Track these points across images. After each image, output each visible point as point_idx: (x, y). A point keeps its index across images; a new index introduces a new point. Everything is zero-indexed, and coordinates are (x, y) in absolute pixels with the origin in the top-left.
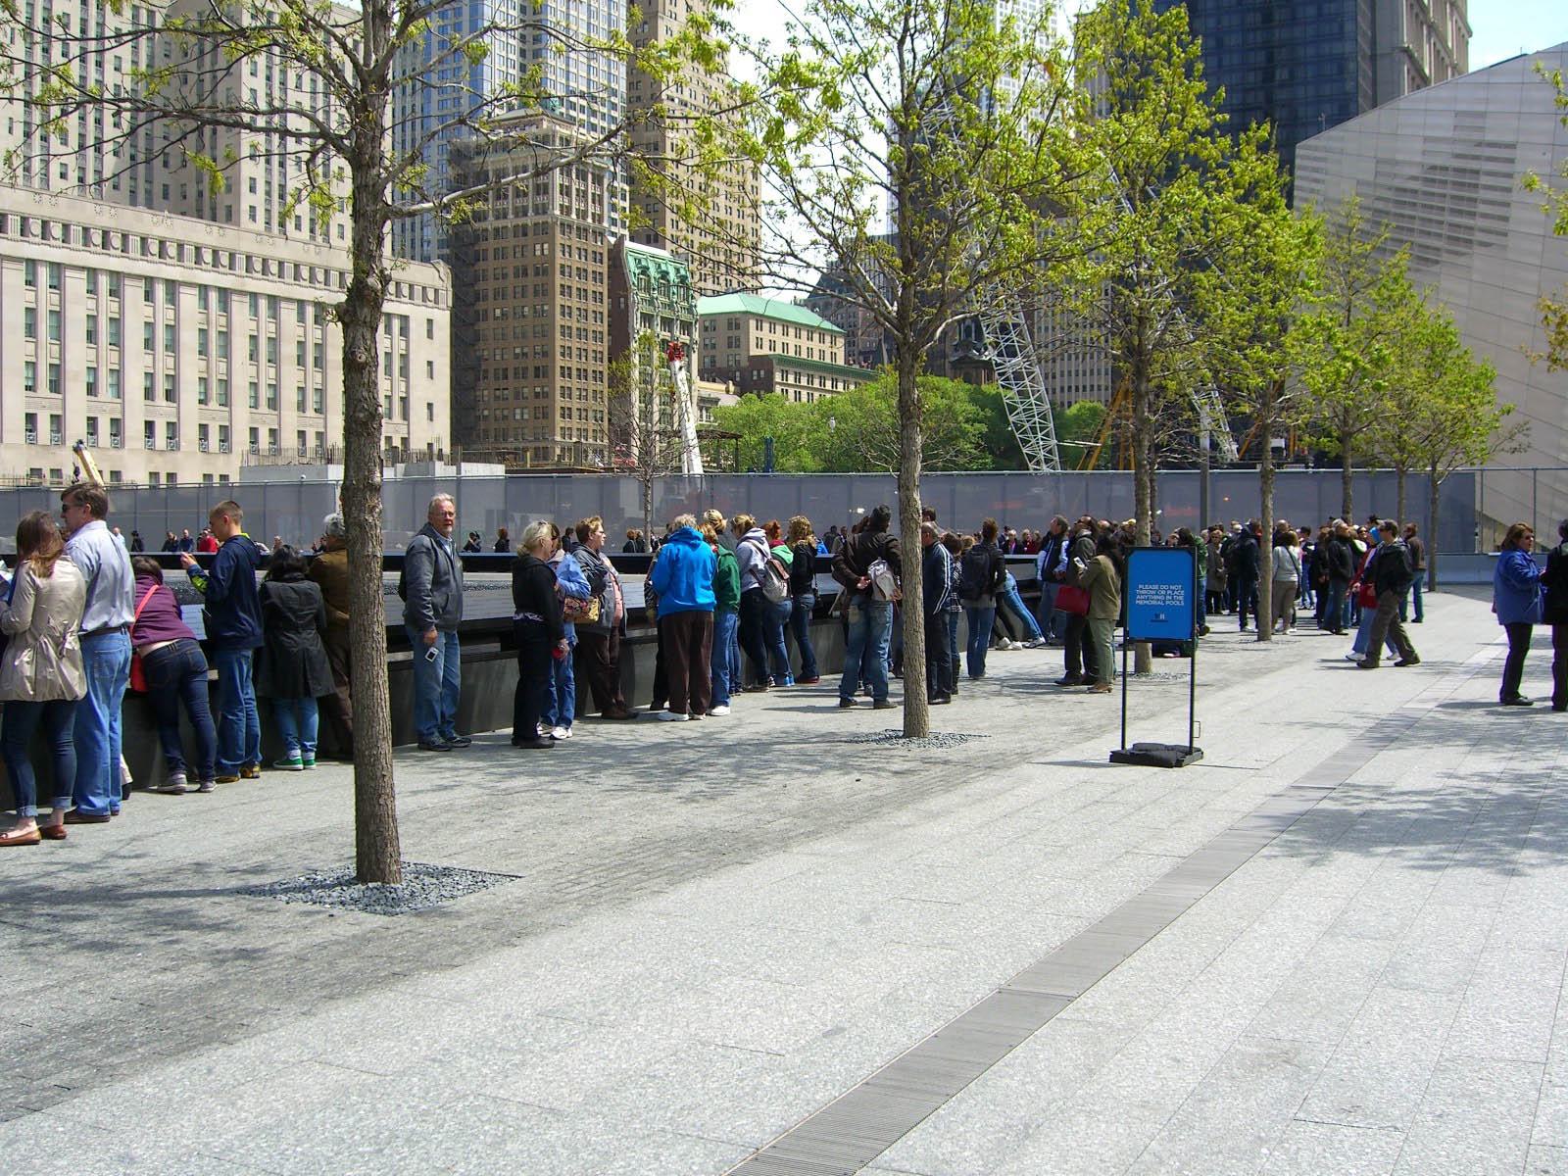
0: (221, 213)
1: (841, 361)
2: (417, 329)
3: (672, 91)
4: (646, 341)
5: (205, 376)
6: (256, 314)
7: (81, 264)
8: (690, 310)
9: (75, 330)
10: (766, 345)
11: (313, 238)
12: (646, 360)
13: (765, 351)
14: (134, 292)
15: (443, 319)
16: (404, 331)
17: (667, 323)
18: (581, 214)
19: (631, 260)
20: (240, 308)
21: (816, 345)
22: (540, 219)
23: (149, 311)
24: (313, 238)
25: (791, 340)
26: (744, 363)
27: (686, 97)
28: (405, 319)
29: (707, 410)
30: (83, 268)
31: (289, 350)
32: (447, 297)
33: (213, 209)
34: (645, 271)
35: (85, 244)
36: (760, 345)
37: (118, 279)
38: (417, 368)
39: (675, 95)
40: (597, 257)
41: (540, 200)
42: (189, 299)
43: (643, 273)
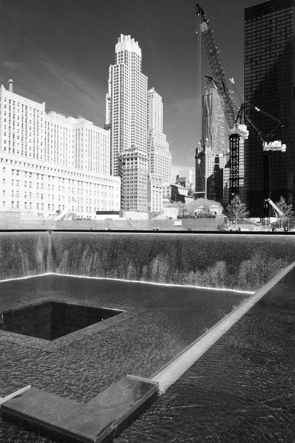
0: (80, 167)
3: (156, 144)
27: (158, 145)
28: (113, 187)
32: (120, 183)
39: (156, 145)
40: (145, 176)
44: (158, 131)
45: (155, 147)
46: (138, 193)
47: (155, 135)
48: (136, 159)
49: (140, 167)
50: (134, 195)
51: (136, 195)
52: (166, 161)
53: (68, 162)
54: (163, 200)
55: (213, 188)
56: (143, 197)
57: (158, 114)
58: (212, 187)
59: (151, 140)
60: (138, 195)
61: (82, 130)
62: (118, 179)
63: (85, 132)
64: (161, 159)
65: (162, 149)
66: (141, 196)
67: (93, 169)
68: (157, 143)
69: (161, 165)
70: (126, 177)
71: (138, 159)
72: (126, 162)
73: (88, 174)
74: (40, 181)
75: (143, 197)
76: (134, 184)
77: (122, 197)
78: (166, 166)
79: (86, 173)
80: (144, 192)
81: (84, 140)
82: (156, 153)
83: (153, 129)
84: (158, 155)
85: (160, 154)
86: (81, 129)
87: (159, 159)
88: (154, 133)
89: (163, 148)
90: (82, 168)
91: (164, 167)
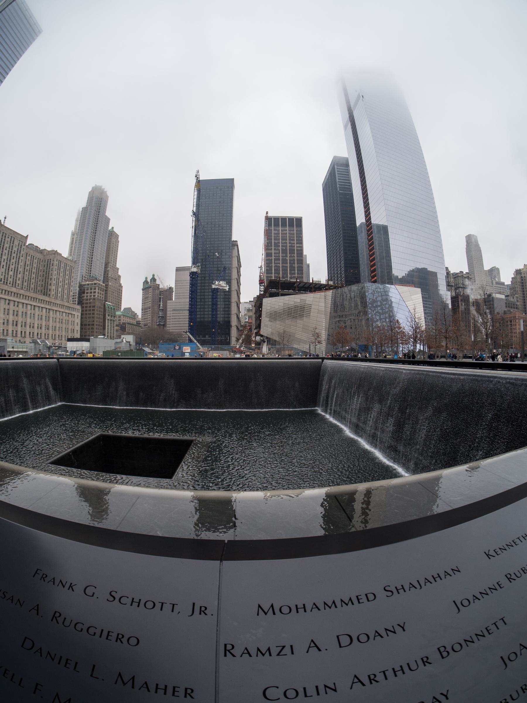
0: (48, 295)
1: (135, 324)
2: (76, 316)
4: (108, 319)
8: (115, 314)
9: (29, 315)
12: (108, 322)
13: (124, 322)
15: (80, 315)
16: (74, 316)
17: (112, 316)
18: (100, 297)
20: (51, 312)
21: (132, 321)
22: (94, 298)
25: (128, 320)
26: (121, 324)
28: (74, 315)
32: (80, 311)
33: (47, 294)
34: (109, 307)
38: (76, 324)
41: (94, 294)
44: (113, 264)
45: (110, 278)
46: (95, 321)
47: (110, 268)
48: (95, 289)
49: (98, 296)
50: (91, 323)
51: (93, 323)
54: (116, 328)
56: (99, 325)
57: (115, 250)
60: (95, 323)
61: (53, 260)
62: (79, 307)
63: (56, 263)
64: (114, 290)
66: (98, 323)
67: (58, 298)
68: (111, 275)
69: (114, 295)
70: (85, 305)
71: (97, 288)
72: (86, 291)
74: (16, 309)
75: (99, 325)
76: (92, 312)
77: (81, 325)
79: (53, 301)
80: (100, 320)
82: (110, 284)
83: (109, 263)
85: (113, 285)
86: (52, 259)
87: (112, 289)
88: (109, 267)
90: (49, 295)
91: (116, 297)
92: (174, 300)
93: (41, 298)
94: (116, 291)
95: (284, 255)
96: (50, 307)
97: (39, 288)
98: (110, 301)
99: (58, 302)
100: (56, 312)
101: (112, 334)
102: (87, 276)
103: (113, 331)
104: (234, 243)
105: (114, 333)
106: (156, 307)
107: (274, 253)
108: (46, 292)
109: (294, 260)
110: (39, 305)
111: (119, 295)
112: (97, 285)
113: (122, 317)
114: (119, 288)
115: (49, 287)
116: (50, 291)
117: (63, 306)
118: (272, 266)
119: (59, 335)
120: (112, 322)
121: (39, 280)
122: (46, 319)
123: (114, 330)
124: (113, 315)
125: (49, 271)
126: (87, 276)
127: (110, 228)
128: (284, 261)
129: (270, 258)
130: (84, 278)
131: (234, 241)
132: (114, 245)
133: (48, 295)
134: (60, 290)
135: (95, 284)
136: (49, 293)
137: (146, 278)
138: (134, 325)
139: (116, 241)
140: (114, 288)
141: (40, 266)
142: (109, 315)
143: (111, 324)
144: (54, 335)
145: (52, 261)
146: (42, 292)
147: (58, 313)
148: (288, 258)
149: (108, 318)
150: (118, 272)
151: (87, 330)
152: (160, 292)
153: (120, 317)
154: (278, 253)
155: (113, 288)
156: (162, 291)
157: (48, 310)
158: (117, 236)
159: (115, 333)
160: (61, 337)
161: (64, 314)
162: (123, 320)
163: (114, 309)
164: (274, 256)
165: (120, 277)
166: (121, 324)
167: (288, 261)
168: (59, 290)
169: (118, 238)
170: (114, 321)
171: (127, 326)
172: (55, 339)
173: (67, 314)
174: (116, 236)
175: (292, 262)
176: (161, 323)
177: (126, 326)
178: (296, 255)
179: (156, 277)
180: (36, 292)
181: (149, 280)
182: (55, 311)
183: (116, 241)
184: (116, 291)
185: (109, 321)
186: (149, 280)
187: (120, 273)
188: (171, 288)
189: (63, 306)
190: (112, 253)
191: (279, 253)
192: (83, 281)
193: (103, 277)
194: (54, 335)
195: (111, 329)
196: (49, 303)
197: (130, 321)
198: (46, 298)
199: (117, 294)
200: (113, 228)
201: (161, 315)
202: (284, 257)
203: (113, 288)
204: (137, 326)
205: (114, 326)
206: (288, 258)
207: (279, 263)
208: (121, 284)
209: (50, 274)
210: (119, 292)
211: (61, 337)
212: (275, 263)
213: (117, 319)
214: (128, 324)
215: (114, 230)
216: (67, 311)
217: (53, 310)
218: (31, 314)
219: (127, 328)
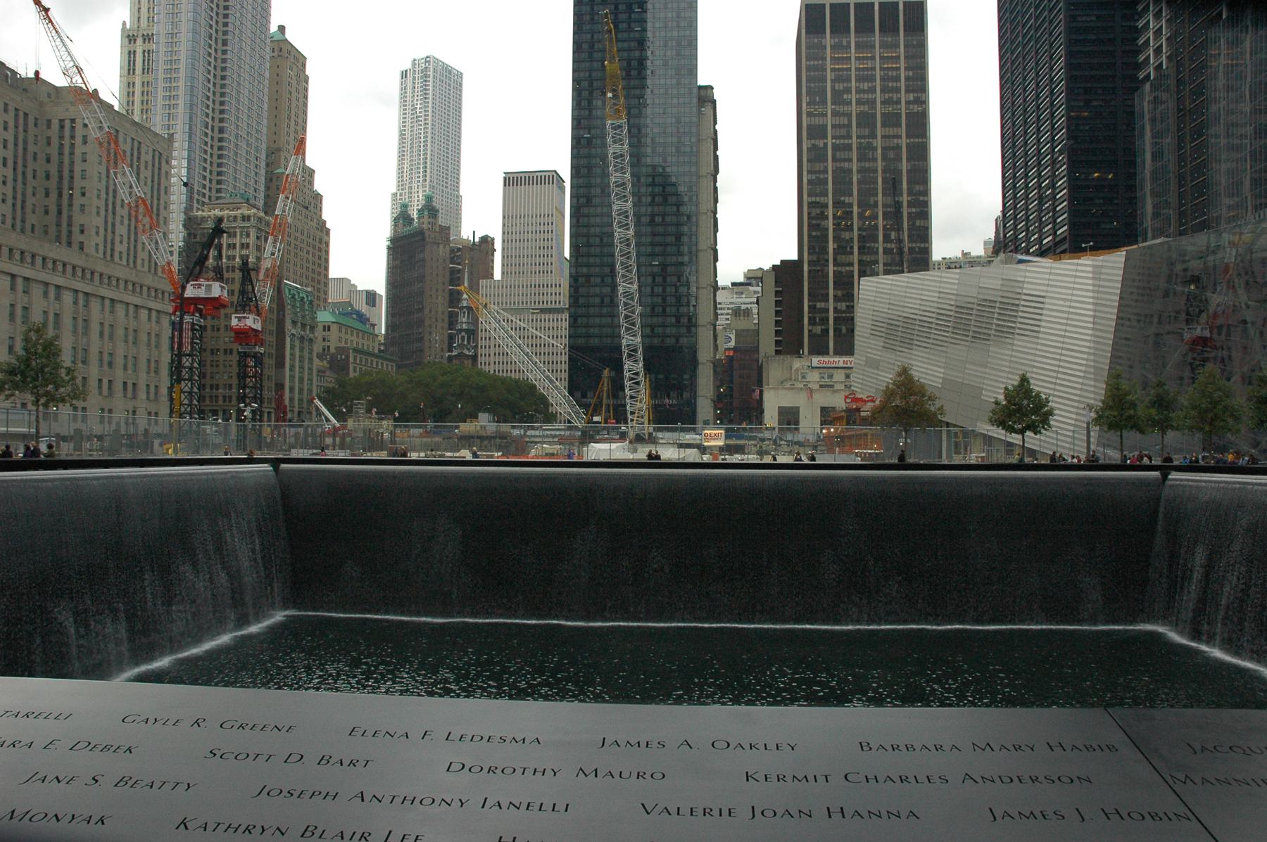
0: (76, 246)
5: (75, 346)
6: (103, 308)
7: (7, 271)
8: (314, 318)
10: (349, 342)
11: (128, 264)
13: (343, 344)
14: (37, 291)
17: (304, 325)
19: (287, 291)
20: (95, 305)
21: (365, 342)
23: (45, 304)
24: (128, 264)
25: (354, 338)
26: (332, 350)
29: (321, 376)
30: (8, 274)
31: (120, 332)
34: (293, 296)
35: (10, 259)
36: (340, 341)
37: (47, 287)
42: (68, 298)
43: (293, 297)
52: (314, 247)
53: (28, 227)
55: (463, 334)
57: (297, 107)
58: (462, 330)
59: (274, 180)
64: (302, 242)
65: (304, 211)
73: (107, 271)
78: (314, 263)
79: (100, 268)
81: (93, 158)
83: (279, 150)
84: (293, 228)
87: (296, 239)
89: (307, 208)
92: (497, 275)
93: (52, 255)
94: (308, 244)
95: (866, 132)
96: (88, 289)
97: (32, 219)
98: (291, 274)
99: (121, 273)
100: (112, 307)
101: (306, 381)
102: (207, 192)
103: (310, 374)
104: (703, 93)
105: (310, 380)
106: (440, 300)
107: (834, 126)
108: (65, 232)
109: (899, 147)
110: (43, 276)
111: (320, 258)
112: (253, 222)
113: (334, 328)
114: (318, 233)
115: (78, 219)
116: (82, 232)
117: (136, 287)
118: (826, 167)
119: (125, 383)
120: (306, 344)
121: (29, 191)
122: (75, 326)
123: (310, 369)
124: (309, 322)
125: (72, 163)
126: (207, 192)
127: (273, 28)
128: (865, 153)
129: (820, 143)
130: (196, 196)
131: (700, 88)
132: (293, 90)
133: (76, 246)
134: (122, 230)
135: (245, 218)
136: (77, 237)
137: (405, 206)
138: (373, 355)
139: (297, 75)
140: (302, 234)
141: (31, 140)
142: (294, 323)
143: (302, 350)
144: (105, 383)
145: (79, 126)
146: (46, 232)
147: (120, 309)
148: (878, 143)
149: (294, 331)
150: (311, 183)
151: (221, 366)
152: (452, 251)
153: (327, 328)
154: (844, 126)
155: (298, 234)
156: (459, 250)
157: (81, 295)
158: (299, 60)
159: (315, 379)
160: (134, 390)
161: (144, 314)
162: (335, 340)
163: (311, 302)
164: (833, 137)
165: (318, 198)
166: (332, 350)
167: (879, 151)
168: (117, 232)
169: (304, 65)
170: (311, 340)
171: (351, 360)
172: (111, 394)
173: (154, 314)
174: (297, 60)
175: (891, 154)
176: (466, 352)
177: (348, 357)
178: (903, 131)
179: (437, 204)
180: (23, 231)
181: (415, 215)
182: (107, 302)
183: (297, 75)
184: (308, 244)
185: (297, 343)
186: (415, 215)
187: (319, 186)
188: (487, 241)
189: (136, 287)
190: (289, 116)
191: (849, 125)
192: (195, 205)
193: (262, 195)
194: (105, 383)
195: (302, 367)
196: (88, 274)
197: (361, 341)
198: (73, 257)
199: (314, 255)
200: (282, 29)
201: (464, 326)
202: (864, 137)
203: (298, 234)
204: (381, 358)
205: (311, 359)
206: (878, 143)
207: (850, 160)
208: (324, 222)
209: (77, 175)
210: (320, 250)
211: (134, 390)
212: (834, 160)
213: (319, 333)
214: (356, 351)
215: (289, 36)
216: (152, 305)
217: (103, 298)
218: (12, 305)
219: (351, 367)
